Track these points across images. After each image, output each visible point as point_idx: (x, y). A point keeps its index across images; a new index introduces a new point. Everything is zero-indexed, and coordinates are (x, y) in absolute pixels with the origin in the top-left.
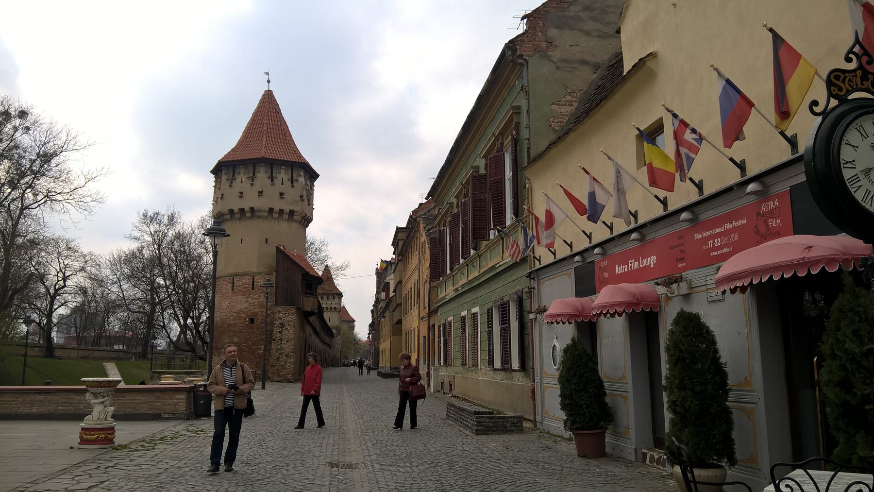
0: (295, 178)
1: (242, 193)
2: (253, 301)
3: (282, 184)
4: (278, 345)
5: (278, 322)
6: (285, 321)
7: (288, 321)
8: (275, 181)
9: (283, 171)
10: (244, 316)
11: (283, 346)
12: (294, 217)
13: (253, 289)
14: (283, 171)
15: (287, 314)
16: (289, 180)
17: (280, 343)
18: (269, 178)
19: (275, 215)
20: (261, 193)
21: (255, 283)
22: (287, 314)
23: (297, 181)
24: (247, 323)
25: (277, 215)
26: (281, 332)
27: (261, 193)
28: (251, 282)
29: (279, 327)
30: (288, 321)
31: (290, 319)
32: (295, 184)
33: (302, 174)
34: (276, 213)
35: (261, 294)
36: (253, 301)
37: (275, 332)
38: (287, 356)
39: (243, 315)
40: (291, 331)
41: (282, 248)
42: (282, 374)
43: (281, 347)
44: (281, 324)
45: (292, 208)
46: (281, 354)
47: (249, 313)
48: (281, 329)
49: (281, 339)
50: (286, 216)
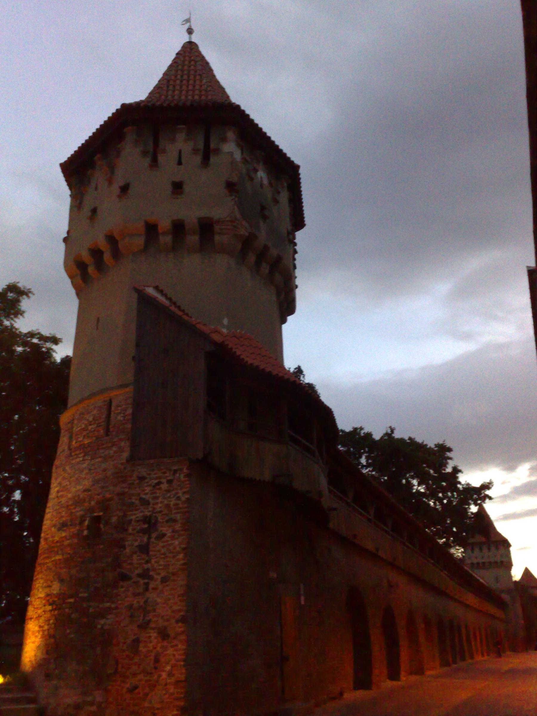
0: (213, 145)
1: (94, 211)
2: (104, 466)
3: (180, 163)
4: (135, 595)
5: (135, 515)
6: (159, 506)
7: (168, 506)
8: (161, 158)
9: (181, 136)
10: (82, 513)
11: (152, 596)
12: (217, 238)
13: (107, 435)
14: (181, 136)
15: (165, 486)
16: (195, 151)
17: (141, 590)
18: (145, 153)
19: (166, 240)
20: (125, 189)
21: (112, 415)
22: (165, 486)
23: (217, 151)
24: (85, 533)
25: (168, 239)
26: (144, 549)
27: (125, 189)
28: (104, 416)
29: (143, 531)
30: (168, 506)
31: (173, 502)
32: (213, 159)
33: (231, 134)
34: (164, 233)
35: (122, 444)
36: (104, 466)
37: (128, 551)
38: (164, 635)
39: (79, 512)
40: (176, 542)
41: (151, 291)
42: (147, 705)
43: (146, 601)
44: (146, 520)
45: (204, 213)
46: (144, 626)
47: (93, 503)
48: (145, 539)
49: (145, 575)
50: (193, 239)
